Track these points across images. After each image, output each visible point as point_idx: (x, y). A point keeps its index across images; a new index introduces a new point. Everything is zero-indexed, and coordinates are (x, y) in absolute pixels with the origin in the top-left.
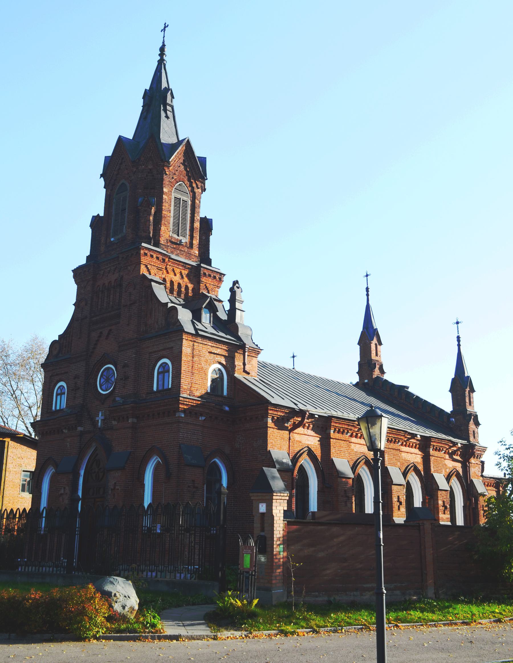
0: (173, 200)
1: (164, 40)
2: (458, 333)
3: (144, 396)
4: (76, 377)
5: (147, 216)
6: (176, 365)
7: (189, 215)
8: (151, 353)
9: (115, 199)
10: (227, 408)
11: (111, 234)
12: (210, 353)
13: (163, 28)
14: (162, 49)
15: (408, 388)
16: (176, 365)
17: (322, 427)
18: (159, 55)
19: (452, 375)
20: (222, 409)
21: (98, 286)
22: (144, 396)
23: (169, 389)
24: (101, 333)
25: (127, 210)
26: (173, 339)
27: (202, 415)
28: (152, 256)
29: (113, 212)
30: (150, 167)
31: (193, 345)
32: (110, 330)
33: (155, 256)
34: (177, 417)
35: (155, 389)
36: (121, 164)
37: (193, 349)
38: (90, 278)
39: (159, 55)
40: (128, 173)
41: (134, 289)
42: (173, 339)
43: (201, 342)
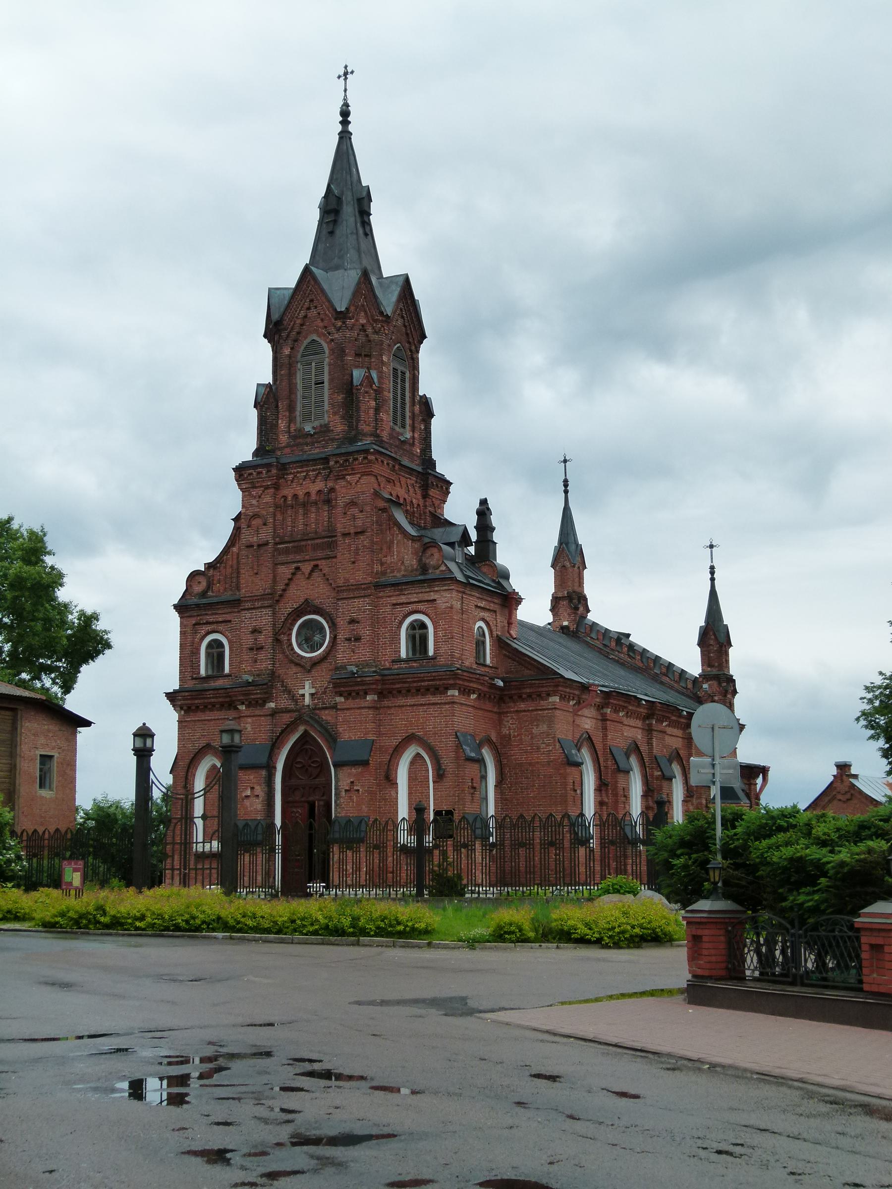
0: (392, 372)
1: (346, 95)
2: (712, 562)
3: (388, 664)
4: (255, 631)
5: (368, 401)
6: (443, 625)
7: (408, 394)
8: (394, 605)
9: (299, 364)
10: (501, 684)
11: (298, 419)
12: (477, 606)
13: (342, 73)
14: (345, 113)
15: (628, 635)
16: (443, 625)
17: (599, 706)
18: (341, 122)
19: (700, 620)
20: (495, 684)
21: (283, 496)
22: (388, 664)
23: (434, 658)
24: (298, 568)
25: (326, 384)
26: (436, 589)
27: (474, 693)
28: (382, 462)
29: (299, 382)
30: (363, 321)
31: (462, 597)
32: (316, 566)
33: (385, 462)
34: (449, 696)
35: (403, 655)
36: (309, 309)
37: (462, 603)
38: (269, 483)
39: (341, 122)
40: (326, 327)
41: (362, 511)
42: (436, 589)
43: (469, 592)
